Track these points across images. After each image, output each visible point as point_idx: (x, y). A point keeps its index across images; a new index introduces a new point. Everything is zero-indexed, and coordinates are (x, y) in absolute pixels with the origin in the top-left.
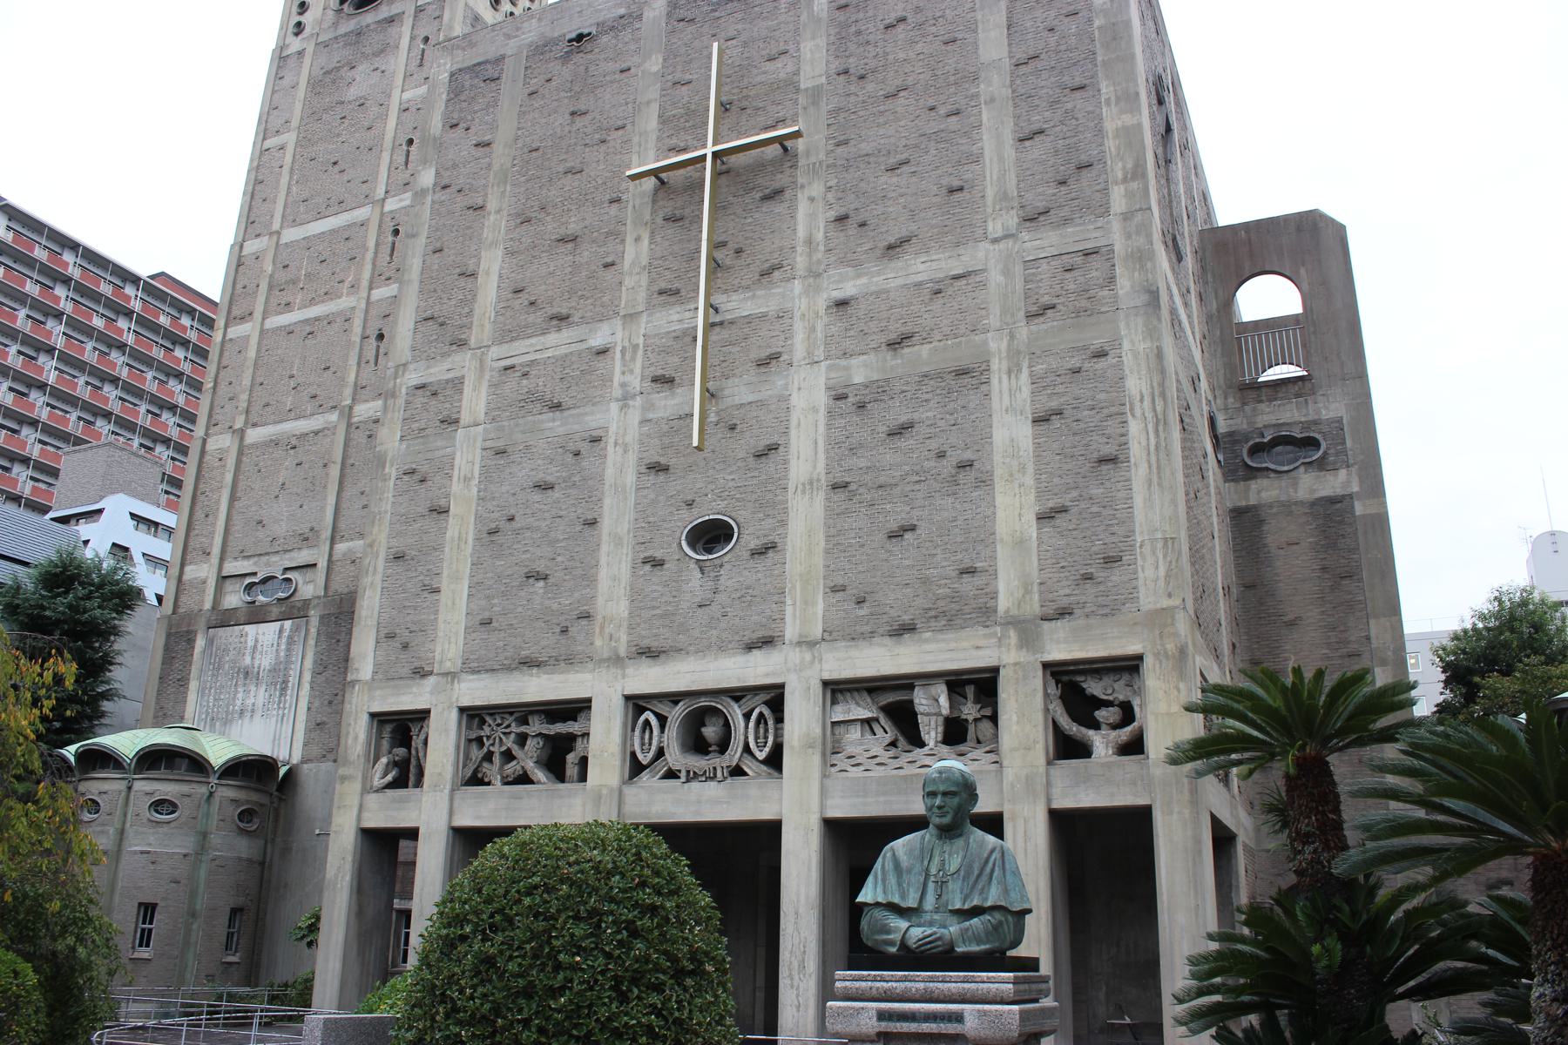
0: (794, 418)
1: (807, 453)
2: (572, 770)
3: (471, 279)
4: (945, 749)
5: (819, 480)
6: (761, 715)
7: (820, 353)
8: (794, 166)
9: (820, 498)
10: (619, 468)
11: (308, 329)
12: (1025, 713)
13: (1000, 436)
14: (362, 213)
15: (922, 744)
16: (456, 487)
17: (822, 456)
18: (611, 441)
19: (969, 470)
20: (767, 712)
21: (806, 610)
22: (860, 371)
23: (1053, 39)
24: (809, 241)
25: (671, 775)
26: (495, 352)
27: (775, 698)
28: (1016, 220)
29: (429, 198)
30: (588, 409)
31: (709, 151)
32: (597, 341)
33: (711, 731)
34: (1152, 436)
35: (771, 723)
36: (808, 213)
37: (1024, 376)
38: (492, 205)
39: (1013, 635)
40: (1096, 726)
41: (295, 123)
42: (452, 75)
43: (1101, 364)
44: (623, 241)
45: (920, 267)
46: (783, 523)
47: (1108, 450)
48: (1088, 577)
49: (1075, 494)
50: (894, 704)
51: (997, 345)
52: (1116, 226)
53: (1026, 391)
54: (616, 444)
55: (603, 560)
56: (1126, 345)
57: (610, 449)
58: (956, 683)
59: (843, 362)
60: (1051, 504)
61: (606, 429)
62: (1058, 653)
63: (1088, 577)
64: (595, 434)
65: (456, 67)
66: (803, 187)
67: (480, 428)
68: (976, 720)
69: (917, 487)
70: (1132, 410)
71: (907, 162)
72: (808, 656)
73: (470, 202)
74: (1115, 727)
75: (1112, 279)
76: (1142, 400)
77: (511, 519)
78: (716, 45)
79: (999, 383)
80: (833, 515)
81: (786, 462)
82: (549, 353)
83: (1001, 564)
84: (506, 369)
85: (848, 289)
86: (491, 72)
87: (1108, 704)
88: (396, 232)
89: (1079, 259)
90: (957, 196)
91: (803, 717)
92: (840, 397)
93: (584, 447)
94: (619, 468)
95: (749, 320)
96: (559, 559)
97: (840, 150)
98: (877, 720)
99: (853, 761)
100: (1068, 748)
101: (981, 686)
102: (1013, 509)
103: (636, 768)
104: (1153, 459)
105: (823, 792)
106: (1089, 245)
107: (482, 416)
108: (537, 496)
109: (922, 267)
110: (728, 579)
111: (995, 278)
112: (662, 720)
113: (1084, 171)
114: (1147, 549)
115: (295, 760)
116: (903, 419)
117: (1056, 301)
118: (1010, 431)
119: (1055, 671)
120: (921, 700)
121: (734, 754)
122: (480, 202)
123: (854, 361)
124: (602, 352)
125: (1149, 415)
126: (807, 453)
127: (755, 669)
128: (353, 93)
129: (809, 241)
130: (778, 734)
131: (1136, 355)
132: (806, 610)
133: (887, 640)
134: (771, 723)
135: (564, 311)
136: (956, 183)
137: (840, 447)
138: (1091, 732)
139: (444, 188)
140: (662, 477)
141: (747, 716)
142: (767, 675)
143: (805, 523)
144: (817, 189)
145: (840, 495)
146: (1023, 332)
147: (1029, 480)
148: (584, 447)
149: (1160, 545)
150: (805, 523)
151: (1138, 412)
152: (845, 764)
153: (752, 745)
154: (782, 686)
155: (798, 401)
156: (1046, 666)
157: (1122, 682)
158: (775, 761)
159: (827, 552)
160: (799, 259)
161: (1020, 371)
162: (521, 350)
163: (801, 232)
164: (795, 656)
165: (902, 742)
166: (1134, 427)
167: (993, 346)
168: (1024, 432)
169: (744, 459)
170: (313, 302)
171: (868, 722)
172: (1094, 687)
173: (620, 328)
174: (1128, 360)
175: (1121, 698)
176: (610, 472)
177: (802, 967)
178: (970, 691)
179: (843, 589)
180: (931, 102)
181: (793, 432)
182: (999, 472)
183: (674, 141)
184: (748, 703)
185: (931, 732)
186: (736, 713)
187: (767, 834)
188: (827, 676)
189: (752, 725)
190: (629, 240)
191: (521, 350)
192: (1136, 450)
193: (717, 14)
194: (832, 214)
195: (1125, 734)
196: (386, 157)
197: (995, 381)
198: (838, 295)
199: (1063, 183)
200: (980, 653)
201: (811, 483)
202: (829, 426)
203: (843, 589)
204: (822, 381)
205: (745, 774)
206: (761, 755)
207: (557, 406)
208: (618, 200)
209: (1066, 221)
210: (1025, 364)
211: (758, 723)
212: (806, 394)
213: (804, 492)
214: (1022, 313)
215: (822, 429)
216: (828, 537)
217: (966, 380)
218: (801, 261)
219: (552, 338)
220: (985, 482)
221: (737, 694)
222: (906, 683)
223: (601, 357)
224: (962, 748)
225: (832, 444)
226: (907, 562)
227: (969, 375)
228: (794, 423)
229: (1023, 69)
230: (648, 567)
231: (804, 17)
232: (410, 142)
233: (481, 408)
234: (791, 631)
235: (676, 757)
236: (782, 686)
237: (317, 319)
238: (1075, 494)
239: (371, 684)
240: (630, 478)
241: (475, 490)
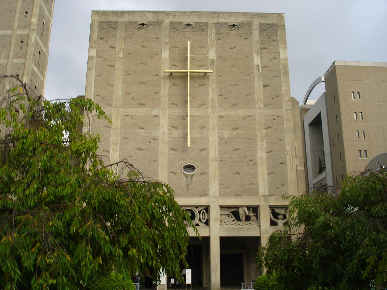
0: (210, 143)
1: (213, 152)
3: (112, 87)
4: (246, 223)
5: (217, 159)
6: (203, 212)
7: (217, 128)
8: (208, 79)
9: (217, 163)
10: (163, 149)
12: (265, 215)
13: (259, 155)
14: (8, 32)
15: (240, 221)
16: (112, 146)
17: (217, 153)
18: (160, 141)
19: (253, 161)
20: (205, 211)
21: (214, 188)
22: (226, 134)
23: (271, 63)
24: (212, 99)
26: (121, 110)
27: (207, 209)
28: (263, 105)
29: (95, 60)
30: (153, 131)
31: (189, 71)
32: (154, 113)
34: (291, 160)
35: (206, 214)
36: (212, 91)
37: (265, 143)
38: (118, 65)
39: (262, 199)
40: (278, 219)
42: (99, 22)
43: (281, 142)
44: (160, 87)
45: (241, 112)
46: (208, 168)
47: (282, 161)
48: (278, 188)
49: (275, 170)
50: (235, 213)
51: (258, 134)
52: (284, 112)
53: (265, 145)
54: (162, 141)
55: (160, 171)
56: (286, 139)
57: (160, 143)
58: (249, 208)
59: (222, 131)
60: (270, 171)
61: (159, 138)
62: (272, 204)
63: (278, 188)
64: (155, 138)
65: (101, 20)
66: (210, 85)
67: (119, 131)
68: (253, 216)
69: (240, 164)
70: (287, 153)
71: (236, 85)
72: (215, 200)
73: (110, 64)
74: (282, 219)
75: (283, 124)
76: (289, 152)
77: (130, 157)
78: (189, 42)
79: (259, 143)
81: (208, 153)
82: (139, 114)
83: (259, 183)
84: (126, 115)
85: (223, 114)
86: (113, 26)
87: (280, 214)
88: (22, 42)
89: (277, 118)
90: (249, 96)
91: (215, 213)
92: (221, 140)
93: (152, 141)
94: (163, 149)
95: (198, 116)
96: (146, 169)
97: (219, 77)
98: (230, 215)
99: (226, 224)
100: (273, 223)
101: (255, 209)
102: (262, 171)
104: (292, 164)
105: (220, 231)
106: (278, 115)
107: (119, 127)
108: (138, 151)
109: (241, 112)
110: (195, 179)
111: (257, 118)
113: (278, 97)
114: (290, 183)
116: (237, 147)
117: (271, 126)
118: (261, 154)
119: (272, 208)
120: (241, 211)
121: (196, 221)
122: (113, 64)
123: (225, 132)
124: (156, 116)
125: (291, 155)
126: (213, 152)
127: (203, 201)
129: (212, 99)
130: (209, 217)
131: (288, 141)
132: (214, 188)
133: (234, 197)
134: (206, 214)
135: (143, 103)
136: (249, 93)
138: (277, 220)
139: (100, 57)
140: (175, 152)
141: (200, 212)
142: (205, 203)
143: (213, 168)
144: (214, 86)
146: (264, 132)
147: (265, 165)
148: (152, 141)
149: (293, 183)
150: (213, 168)
151: (289, 154)
152: (224, 224)
153: (201, 219)
154: (209, 206)
155: (211, 139)
156: (269, 206)
157: (283, 210)
158: (207, 223)
159: (219, 176)
160: (210, 103)
161: (263, 141)
162: (131, 111)
163: (210, 96)
164: (212, 199)
165: (236, 220)
166: (288, 157)
167: (257, 134)
168: (264, 155)
169: (197, 151)
171: (228, 215)
172: (277, 211)
173: (161, 111)
174: (286, 142)
175: (283, 213)
176: (160, 149)
177: (216, 269)
178: (251, 210)
179: (223, 185)
181: (210, 146)
182: (258, 163)
183: (174, 63)
184: (199, 209)
185: (243, 217)
186: (196, 211)
187: (207, 240)
188: (220, 204)
189: (201, 214)
190: (162, 87)
191: (131, 111)
192: (288, 162)
193: (184, 30)
194: (218, 94)
195: (284, 221)
196: (17, 16)
197: (258, 142)
198: (220, 114)
199: (273, 99)
200: (256, 202)
201: (215, 159)
202: (219, 146)
203: (223, 185)
204: (217, 135)
205: (199, 225)
206: (204, 221)
207: (141, 128)
208: (158, 75)
209: (274, 108)
210: (265, 139)
211: (202, 214)
212: (213, 137)
213: (213, 161)
214: (264, 128)
215: (217, 146)
216: (219, 172)
217: (251, 140)
218: (210, 104)
219: (140, 110)
220: (256, 164)
221: (196, 207)
222: (238, 207)
223: (156, 118)
224: (250, 222)
226: (238, 180)
227: (252, 139)
228: (210, 144)
229: (264, 69)
230: (172, 174)
231: (209, 39)
232: (27, 13)
233: (119, 124)
234: (211, 193)
236: (209, 206)
238: (275, 170)
240: (166, 151)
241: (118, 147)
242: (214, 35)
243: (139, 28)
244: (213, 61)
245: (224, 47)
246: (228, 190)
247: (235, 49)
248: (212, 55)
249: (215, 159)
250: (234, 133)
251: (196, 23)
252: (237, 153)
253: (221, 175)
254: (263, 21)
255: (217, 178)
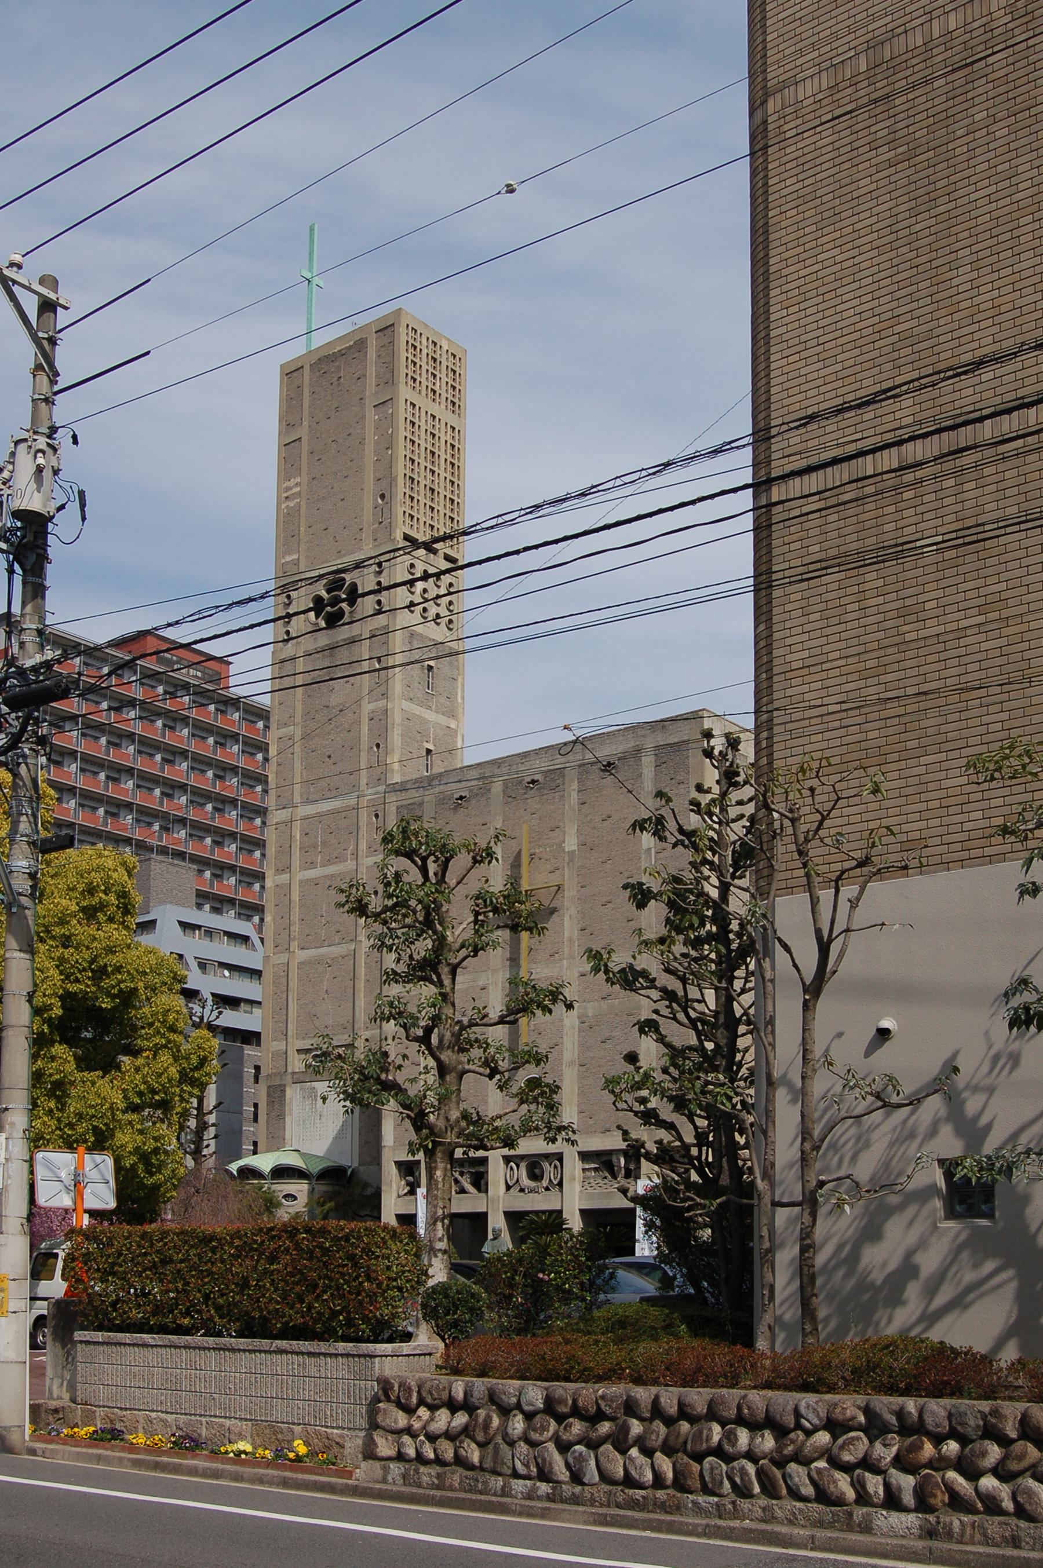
2: (483, 1188)
11: (329, 883)
25: (522, 1190)
32: (481, 983)
33: (537, 1171)
41: (298, 718)
80: (581, 1077)
103: (508, 1187)
112: (518, 1166)
115: (356, 1164)
123: (590, 1005)
128: (334, 700)
129: (570, 940)
137: (583, 1046)
145: (582, 1069)
163: (566, 934)
170: (330, 862)
180: (621, 869)
222: (610, 1153)
225: (581, 1045)
229: (660, 855)
235: (526, 1182)
237: (333, 876)
239: (394, 1148)
242: (574, 795)
243: (455, 809)
244: (572, 853)
245: (590, 822)
246: (591, 1122)
247: (610, 820)
248: (571, 843)
249: (572, 1062)
250: (605, 1005)
251: (545, 773)
252: (607, 1046)
253: (582, 1093)
254: (661, 739)
255: (575, 1099)
